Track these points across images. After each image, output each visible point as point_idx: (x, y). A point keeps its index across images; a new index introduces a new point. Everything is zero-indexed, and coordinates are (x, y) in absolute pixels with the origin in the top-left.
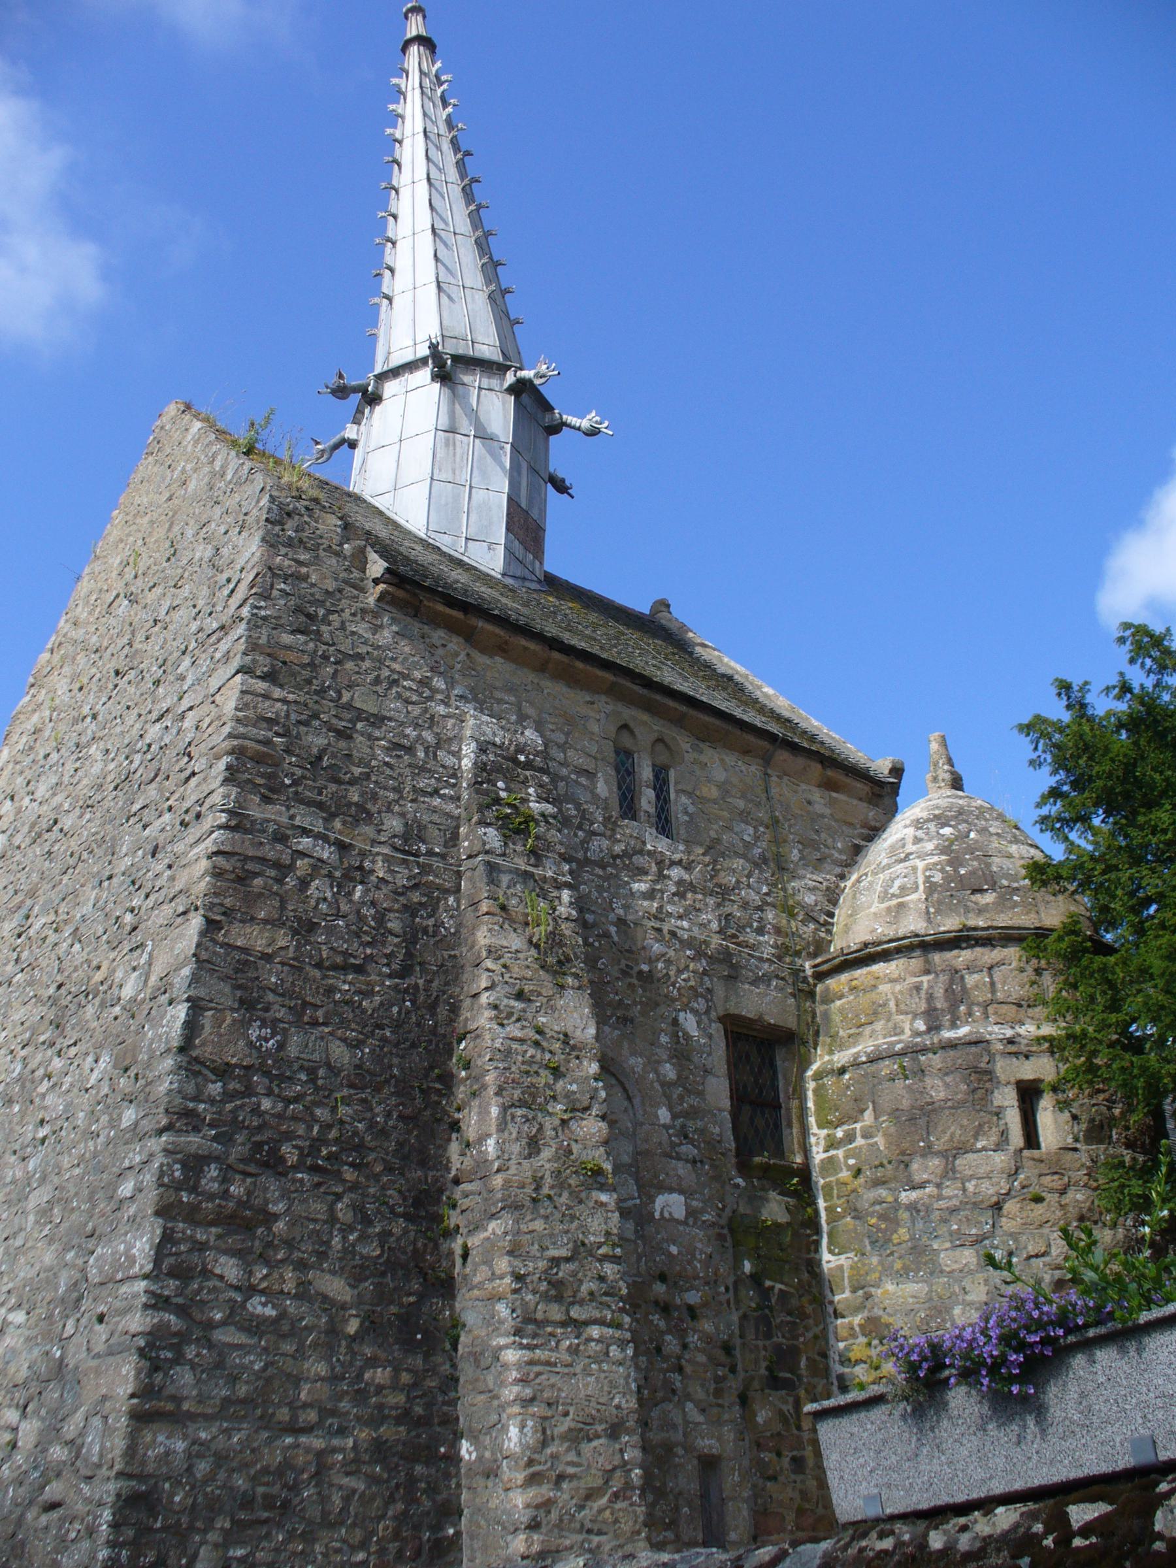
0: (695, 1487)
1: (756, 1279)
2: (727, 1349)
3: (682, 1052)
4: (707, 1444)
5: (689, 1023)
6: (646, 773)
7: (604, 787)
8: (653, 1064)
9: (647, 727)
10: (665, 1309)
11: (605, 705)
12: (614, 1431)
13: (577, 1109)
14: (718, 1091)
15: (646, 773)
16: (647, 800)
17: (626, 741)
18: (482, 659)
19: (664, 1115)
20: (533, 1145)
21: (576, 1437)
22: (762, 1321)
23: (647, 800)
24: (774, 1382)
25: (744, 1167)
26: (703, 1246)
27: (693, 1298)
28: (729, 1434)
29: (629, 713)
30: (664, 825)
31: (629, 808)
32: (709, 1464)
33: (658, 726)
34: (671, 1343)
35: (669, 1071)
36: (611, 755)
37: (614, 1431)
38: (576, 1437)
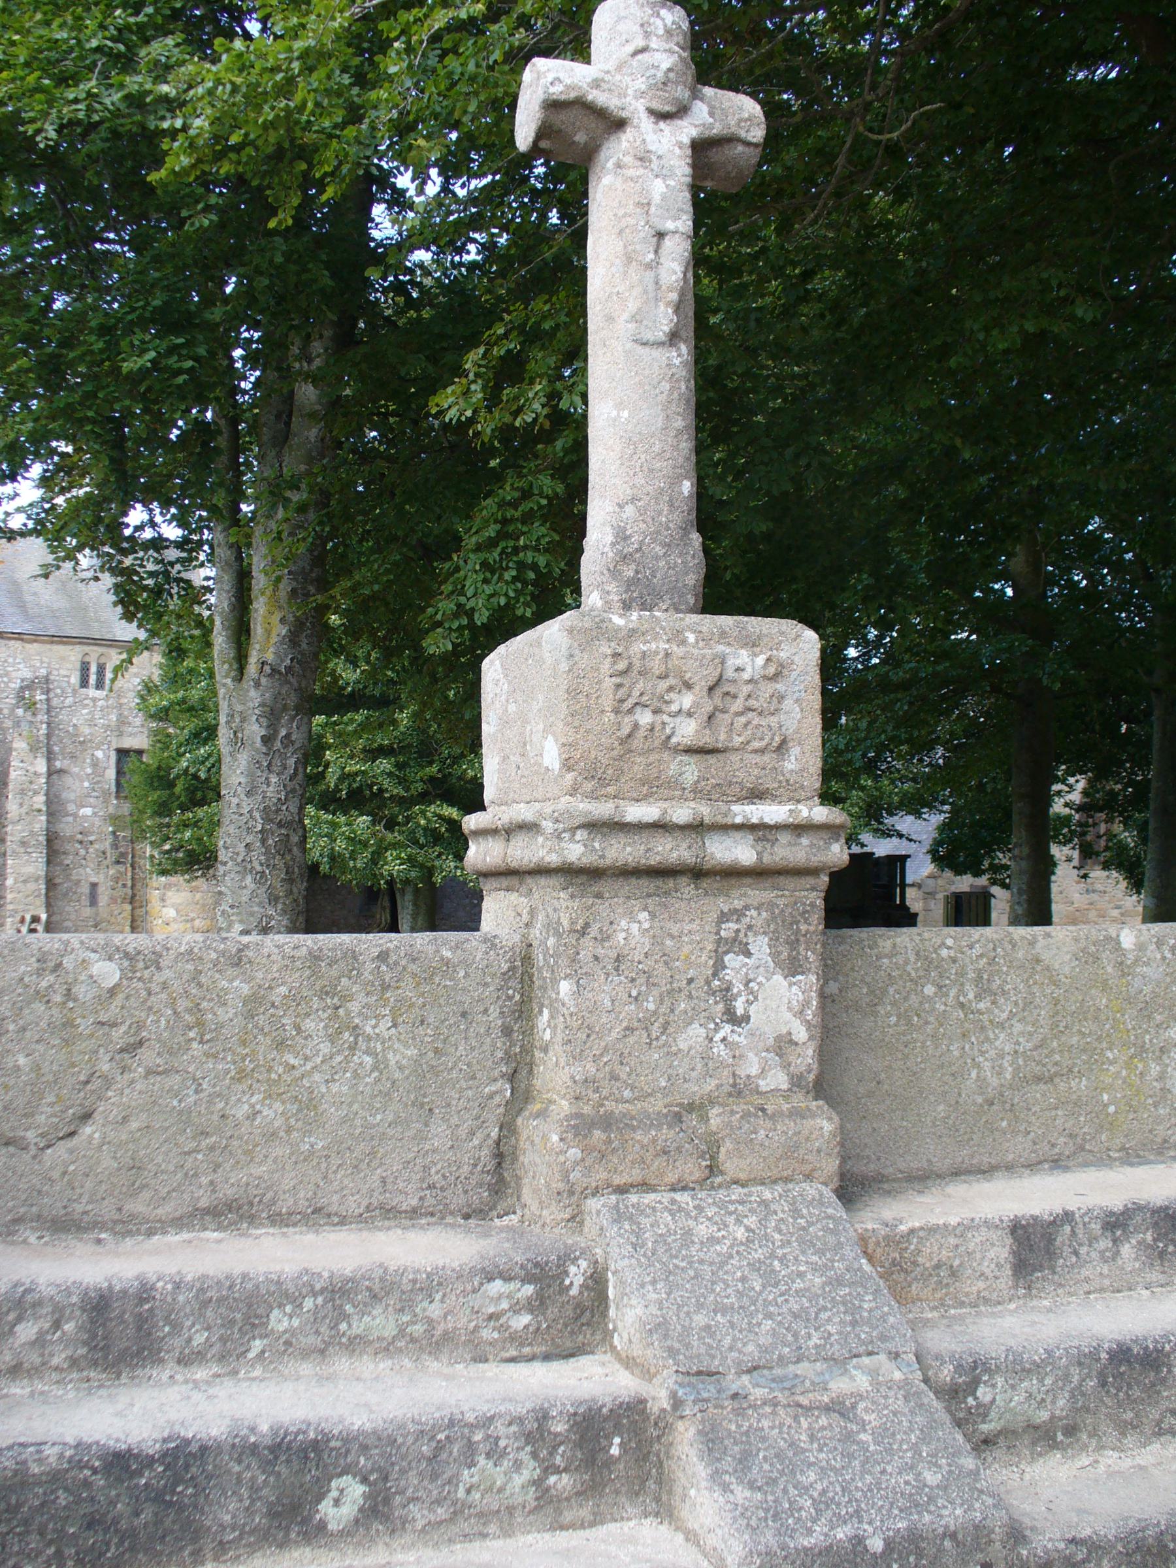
0: (87, 891)
1: (114, 833)
2: (104, 853)
3: (95, 764)
4: (94, 880)
5: (99, 754)
6: (93, 669)
7: (75, 679)
8: (83, 769)
9: (94, 653)
10: (81, 842)
11: (78, 648)
12: (37, 880)
13: (36, 793)
14: (111, 774)
15: (93, 669)
16: (93, 679)
17: (87, 659)
18: (28, 646)
19: (86, 784)
20: (21, 805)
21: (25, 882)
22: (115, 846)
23: (93, 679)
24: (118, 862)
25: (117, 797)
26: (97, 822)
27: (92, 838)
28: (102, 876)
29: (87, 649)
30: (100, 685)
31: (84, 683)
32: (94, 885)
33: (100, 650)
34: (82, 852)
35: (89, 771)
36: (78, 665)
37: (37, 880)
38: (25, 882)
